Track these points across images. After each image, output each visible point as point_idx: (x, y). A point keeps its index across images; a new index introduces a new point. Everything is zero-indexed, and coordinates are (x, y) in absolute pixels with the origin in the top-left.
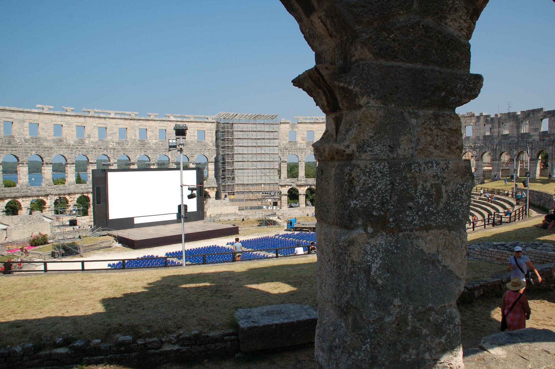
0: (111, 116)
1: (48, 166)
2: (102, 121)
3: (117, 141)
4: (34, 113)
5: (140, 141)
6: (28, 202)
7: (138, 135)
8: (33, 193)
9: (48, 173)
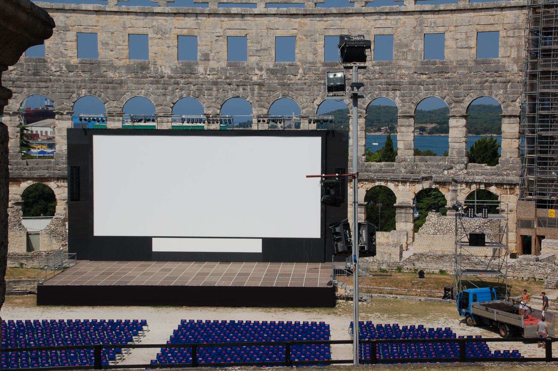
0: (256, 11)
2: (237, 22)
3: (271, 67)
4: (87, 12)
5: (325, 64)
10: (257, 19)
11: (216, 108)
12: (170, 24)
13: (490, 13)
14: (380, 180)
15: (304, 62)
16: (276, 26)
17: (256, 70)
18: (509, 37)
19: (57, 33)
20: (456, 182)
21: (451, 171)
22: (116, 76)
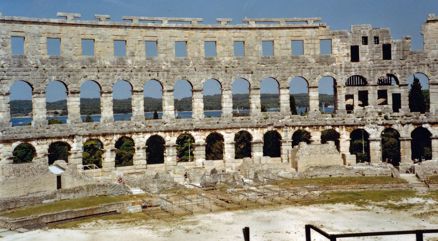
0: (163, 25)
1: (74, 97)
2: (151, 32)
3: (173, 60)
4: (54, 24)
5: (206, 59)
6: (45, 145)
7: (203, 50)
8: (53, 133)
9: (75, 106)
10: (163, 30)
11: (141, 86)
12: (108, 33)
13: (297, 30)
14: (243, 128)
15: (193, 57)
16: (175, 35)
18: (309, 43)
19: (33, 38)
20: (287, 126)
21: (283, 120)
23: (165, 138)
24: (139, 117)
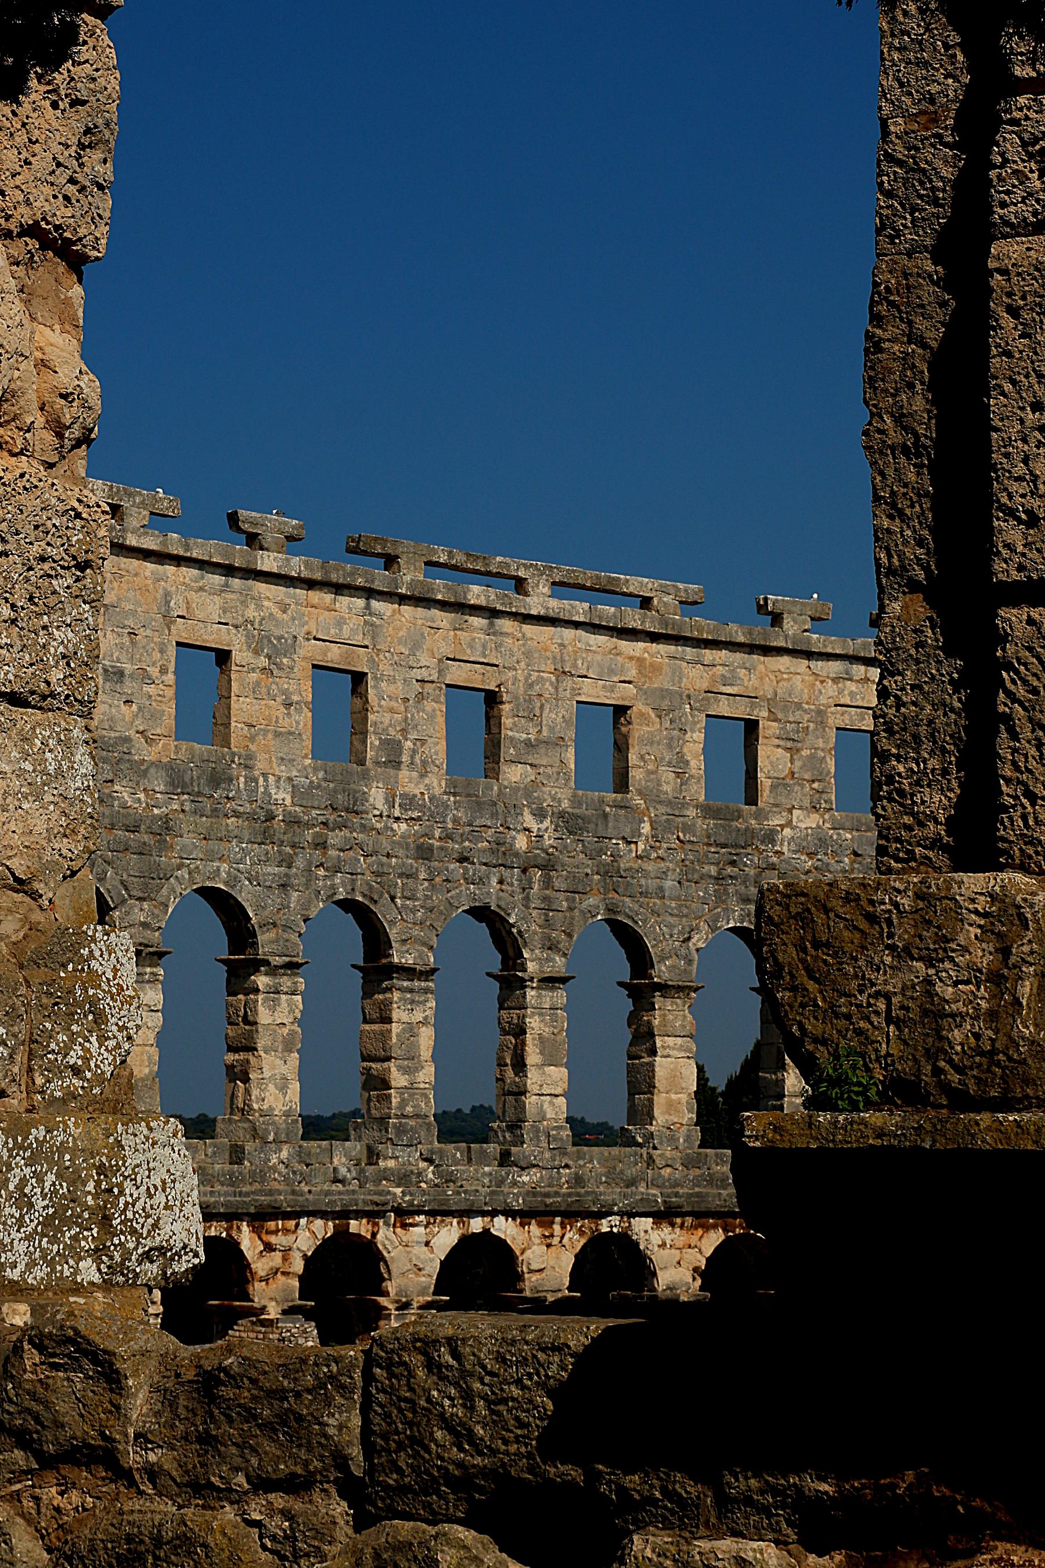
5: (708, 811)
7: (696, 765)
11: (424, 944)
12: (293, 619)
17: (526, 812)
22: (139, 799)
23: (522, 1253)
24: (412, 1123)
